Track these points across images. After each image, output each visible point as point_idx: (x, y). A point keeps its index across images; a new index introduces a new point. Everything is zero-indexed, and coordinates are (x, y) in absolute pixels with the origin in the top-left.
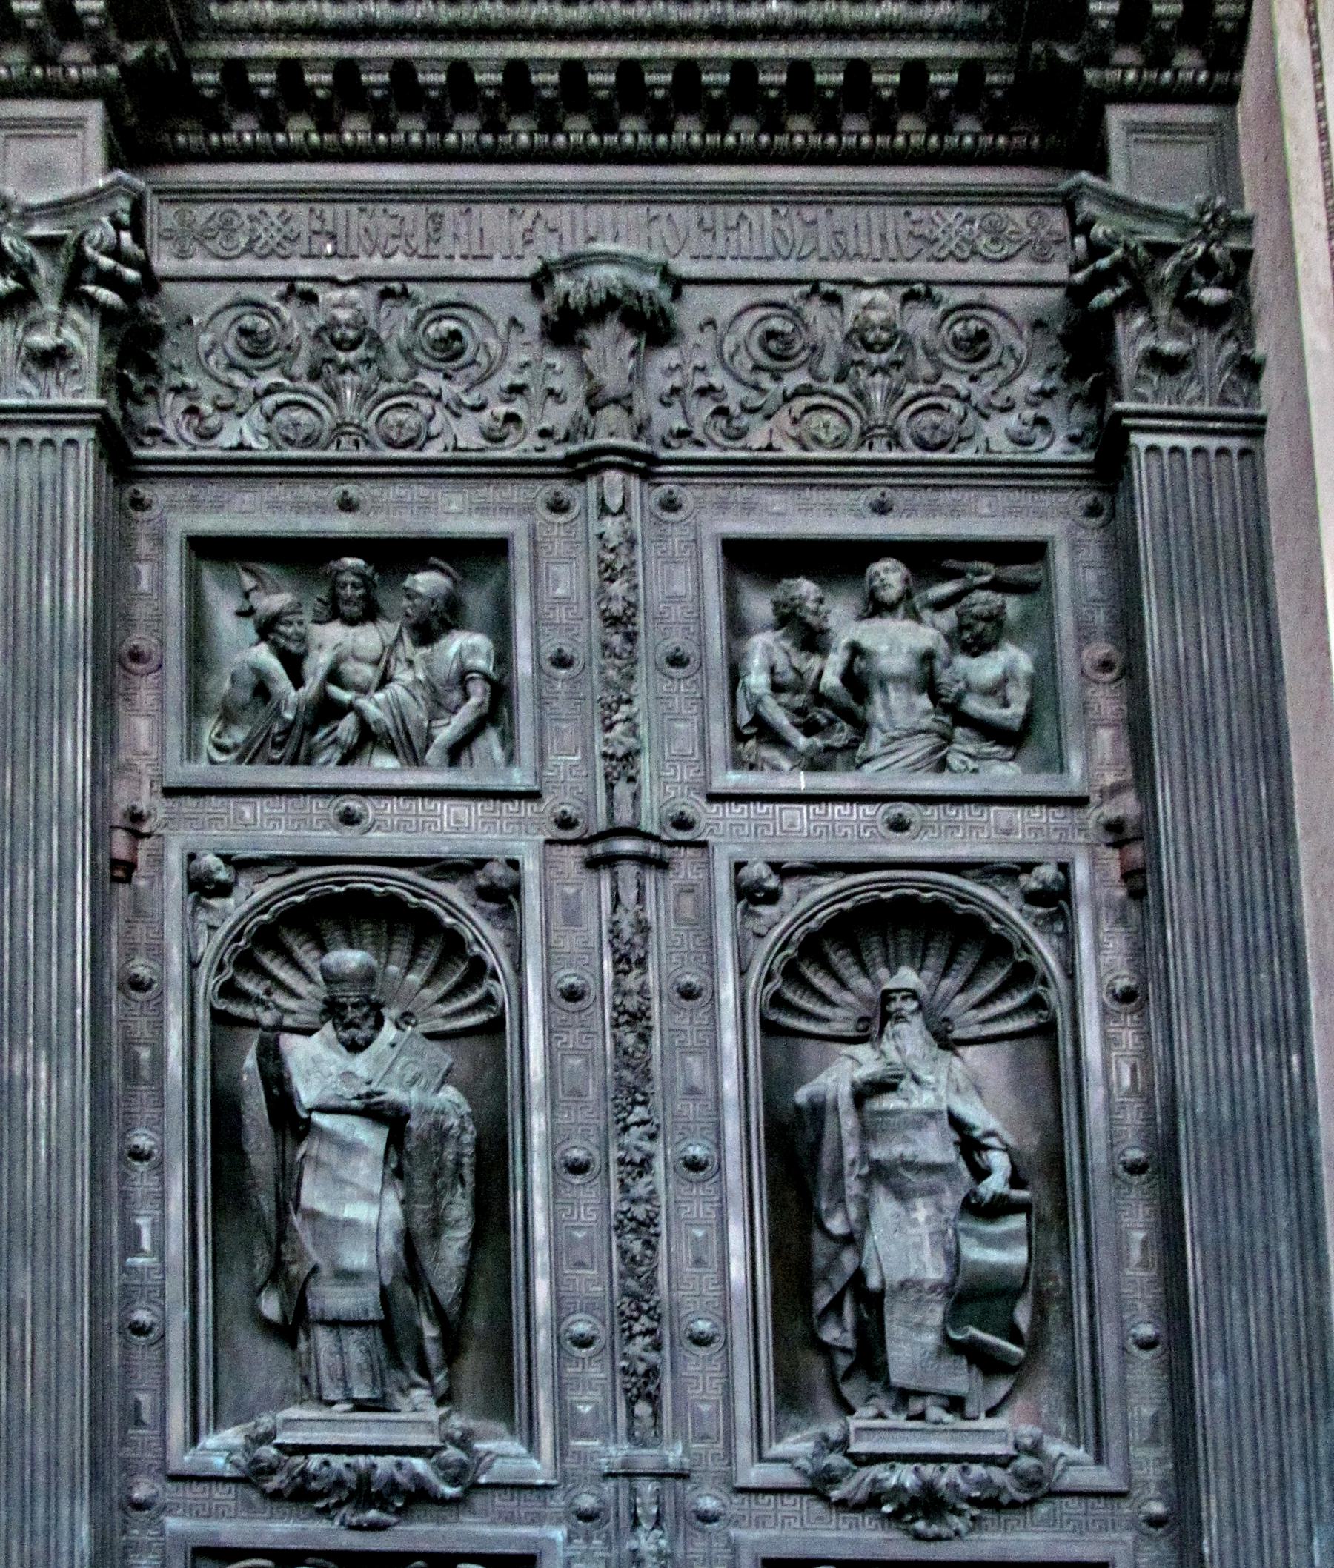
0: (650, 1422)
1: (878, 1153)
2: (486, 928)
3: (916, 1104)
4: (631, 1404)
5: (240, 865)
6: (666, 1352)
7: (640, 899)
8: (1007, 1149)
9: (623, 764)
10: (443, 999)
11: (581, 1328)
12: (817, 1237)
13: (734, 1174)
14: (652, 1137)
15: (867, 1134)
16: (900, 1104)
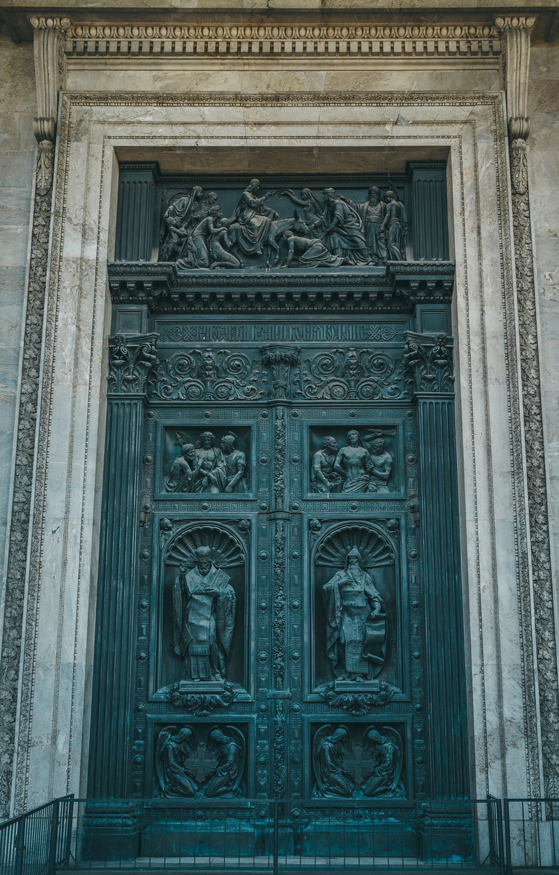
0: (281, 683)
1: (345, 603)
2: (241, 538)
3: (355, 589)
4: (276, 678)
5: (173, 522)
6: (286, 662)
7: (283, 531)
8: (380, 602)
9: (279, 493)
10: (228, 557)
11: (263, 655)
12: (328, 627)
13: (306, 609)
14: (284, 599)
15: (344, 596)
16: (351, 589)
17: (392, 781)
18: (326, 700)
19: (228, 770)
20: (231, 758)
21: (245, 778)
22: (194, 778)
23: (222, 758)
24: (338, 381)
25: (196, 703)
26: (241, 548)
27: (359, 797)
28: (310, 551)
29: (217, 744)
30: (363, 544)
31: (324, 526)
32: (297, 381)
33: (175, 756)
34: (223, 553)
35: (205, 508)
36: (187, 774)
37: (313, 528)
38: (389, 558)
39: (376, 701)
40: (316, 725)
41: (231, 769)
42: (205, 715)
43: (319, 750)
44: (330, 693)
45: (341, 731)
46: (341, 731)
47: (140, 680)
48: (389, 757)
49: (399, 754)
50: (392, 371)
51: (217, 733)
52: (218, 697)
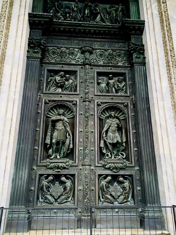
5: (49, 101)
17: (128, 197)
18: (104, 166)
19: (67, 193)
20: (68, 188)
21: (74, 196)
22: (53, 197)
23: (65, 188)
24: (105, 59)
25: (56, 166)
26: (74, 111)
27: (116, 204)
28: (97, 113)
29: (63, 183)
30: (115, 112)
31: (102, 105)
32: (92, 59)
33: (46, 188)
34: (67, 113)
35: (61, 97)
36: (51, 195)
37: (99, 105)
38: (125, 116)
39: (122, 167)
40: (100, 175)
41: (69, 193)
42: (59, 172)
43: (101, 185)
44: (106, 163)
45: (109, 178)
46: (109, 178)
47: (34, 158)
48: (128, 188)
49: (131, 187)
50: (123, 57)
51: (63, 179)
52: (64, 164)
